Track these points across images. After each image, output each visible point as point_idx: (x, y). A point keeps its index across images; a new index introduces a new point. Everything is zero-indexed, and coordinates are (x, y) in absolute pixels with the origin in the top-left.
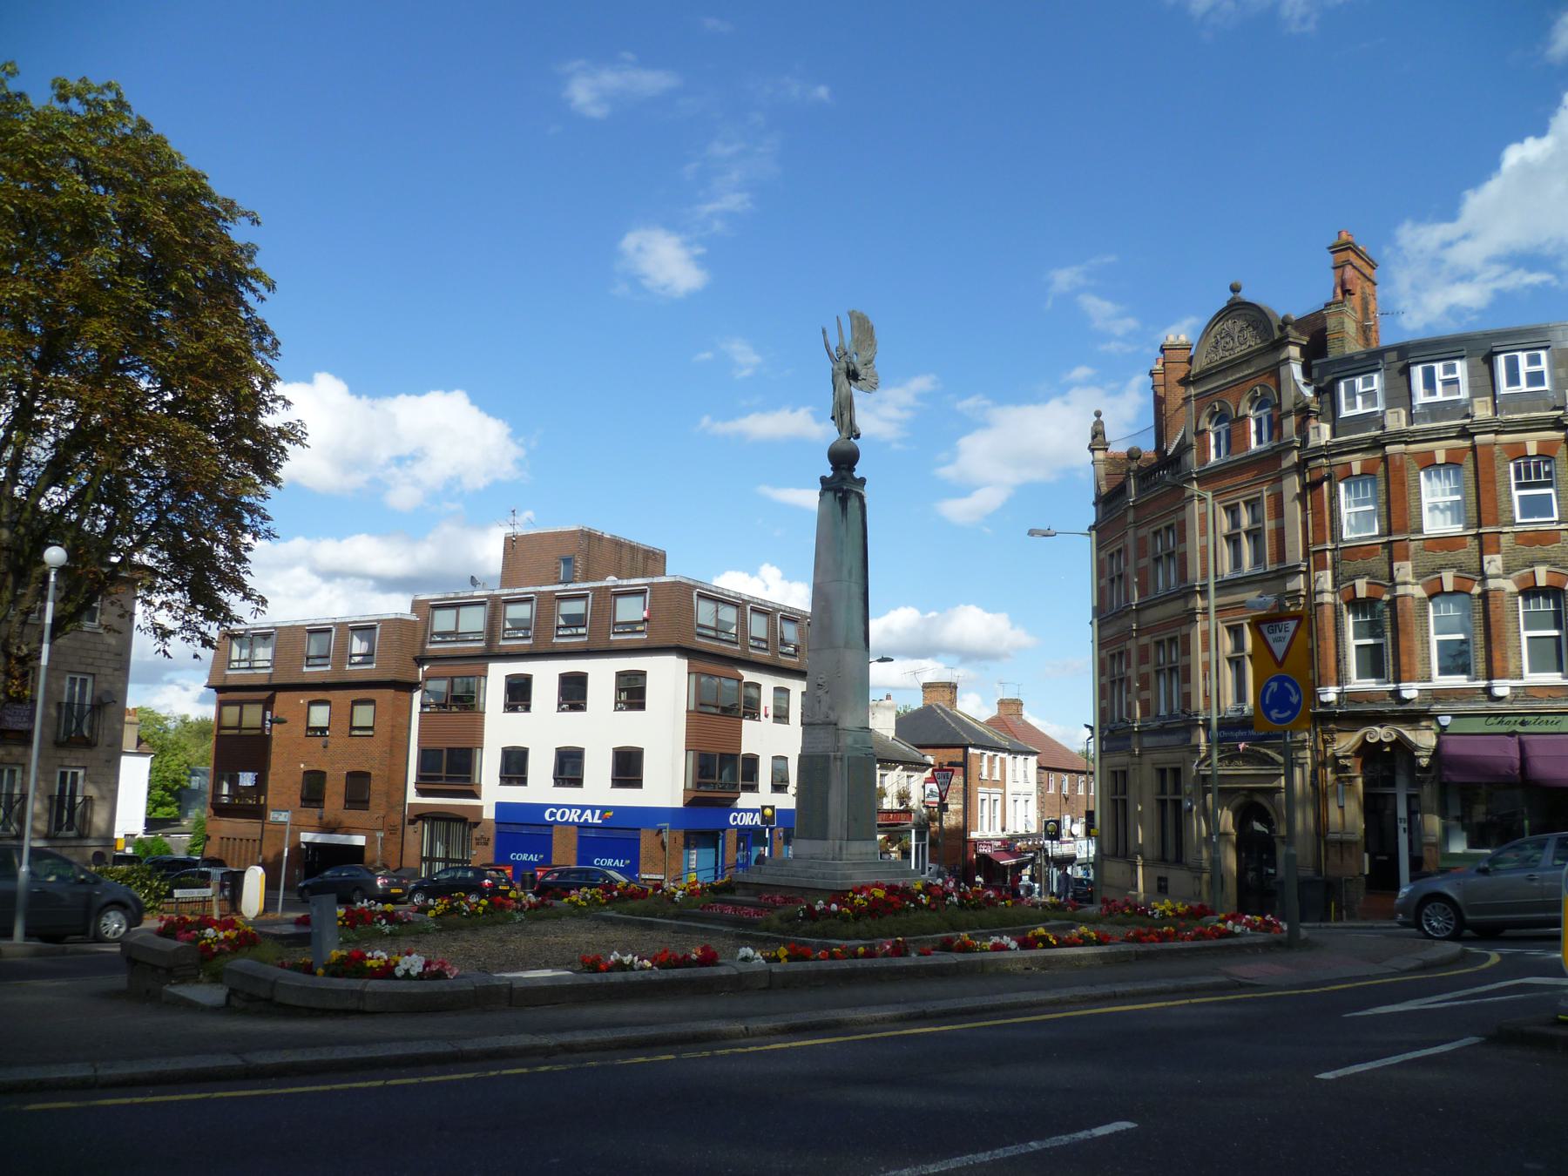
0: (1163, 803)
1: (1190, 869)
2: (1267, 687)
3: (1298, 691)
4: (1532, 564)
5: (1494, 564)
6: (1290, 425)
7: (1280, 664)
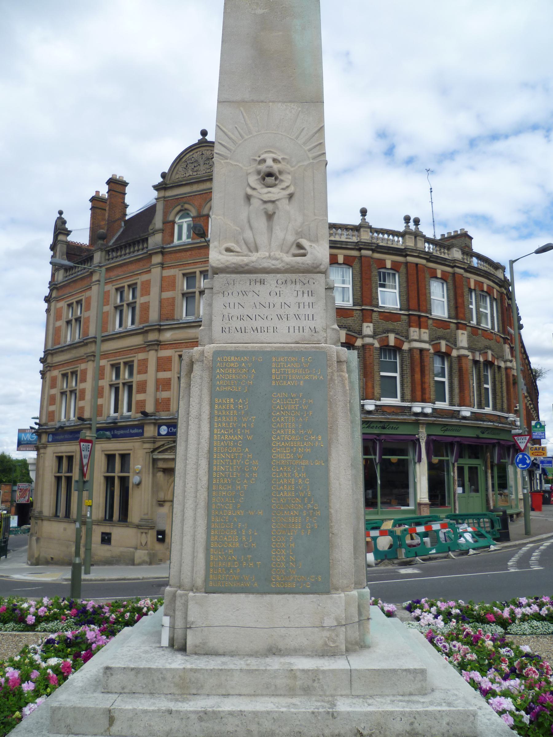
0: (109, 481)
1: (138, 527)
4: (388, 331)
5: (368, 329)
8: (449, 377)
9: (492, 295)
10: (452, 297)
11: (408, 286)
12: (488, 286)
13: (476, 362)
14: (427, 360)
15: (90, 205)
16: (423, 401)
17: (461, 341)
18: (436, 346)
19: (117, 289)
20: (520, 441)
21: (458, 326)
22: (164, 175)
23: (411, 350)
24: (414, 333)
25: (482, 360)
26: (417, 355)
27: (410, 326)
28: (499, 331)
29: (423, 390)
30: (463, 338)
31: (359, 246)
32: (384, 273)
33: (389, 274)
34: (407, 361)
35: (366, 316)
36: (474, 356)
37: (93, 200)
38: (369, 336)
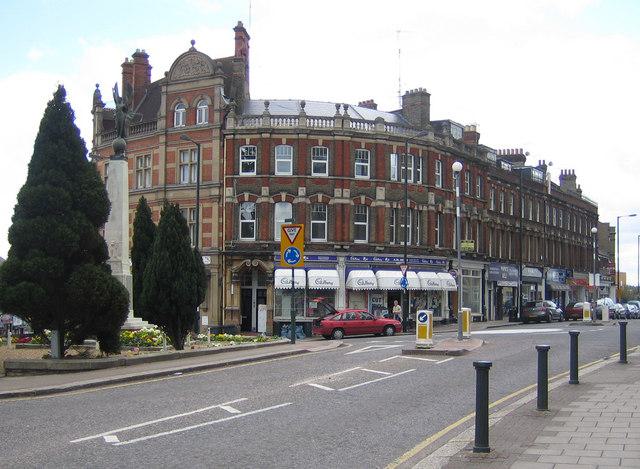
5: (302, 191)
6: (217, 116)
15: (121, 70)
18: (357, 201)
19: (138, 158)
21: (378, 184)
22: (166, 74)
23: (334, 205)
26: (339, 208)
29: (343, 233)
30: (381, 193)
31: (297, 131)
35: (301, 182)
37: (124, 65)
38: (302, 197)
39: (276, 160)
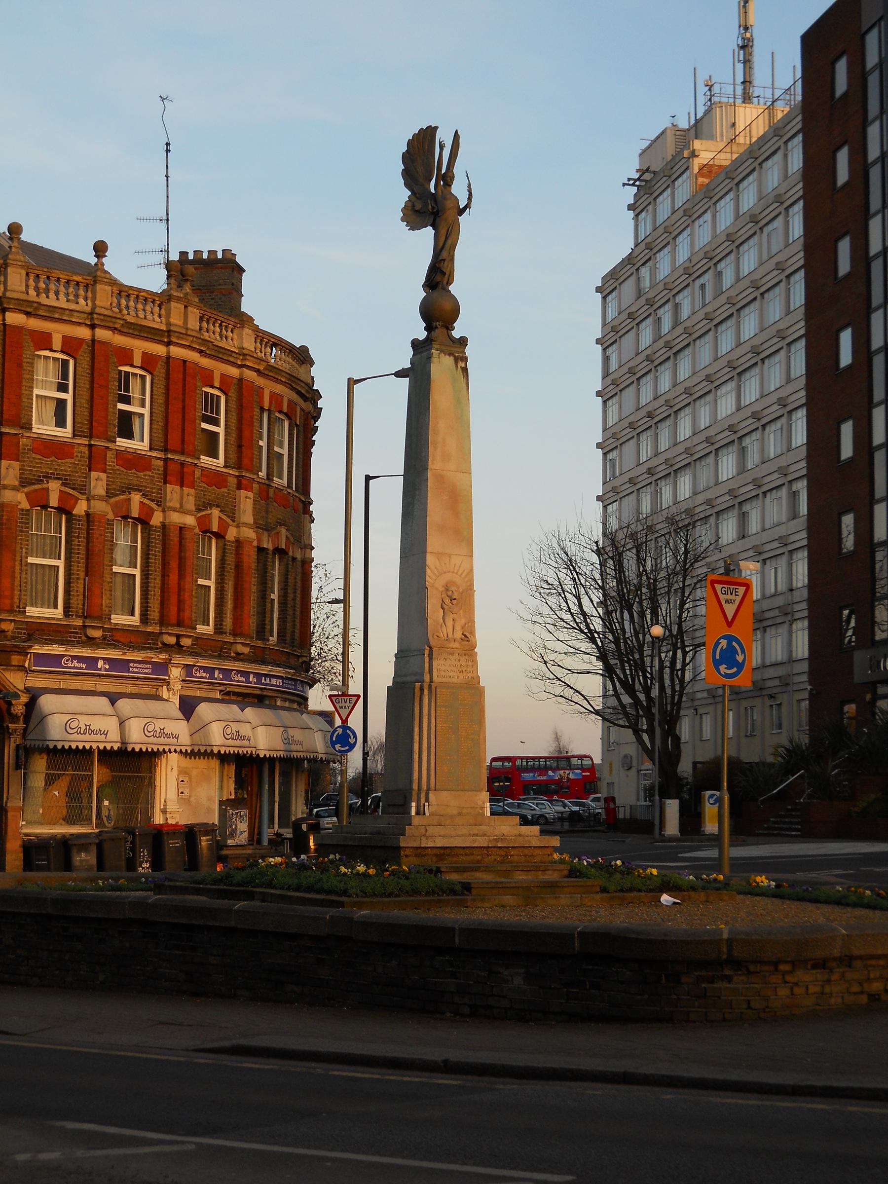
2: (718, 643)
3: (743, 651)
4: (129, 489)
5: (98, 483)
7: (730, 624)
8: (216, 579)
9: (293, 419)
10: (233, 427)
11: (167, 403)
12: (290, 401)
13: (261, 550)
14: (190, 546)
16: (179, 624)
17: (244, 512)
20: (340, 704)
24: (172, 492)
25: (271, 547)
27: (165, 482)
28: (297, 490)
32: (127, 373)
33: (135, 375)
34: (157, 548)
36: (259, 540)
38: (100, 498)
39: (36, 391)
